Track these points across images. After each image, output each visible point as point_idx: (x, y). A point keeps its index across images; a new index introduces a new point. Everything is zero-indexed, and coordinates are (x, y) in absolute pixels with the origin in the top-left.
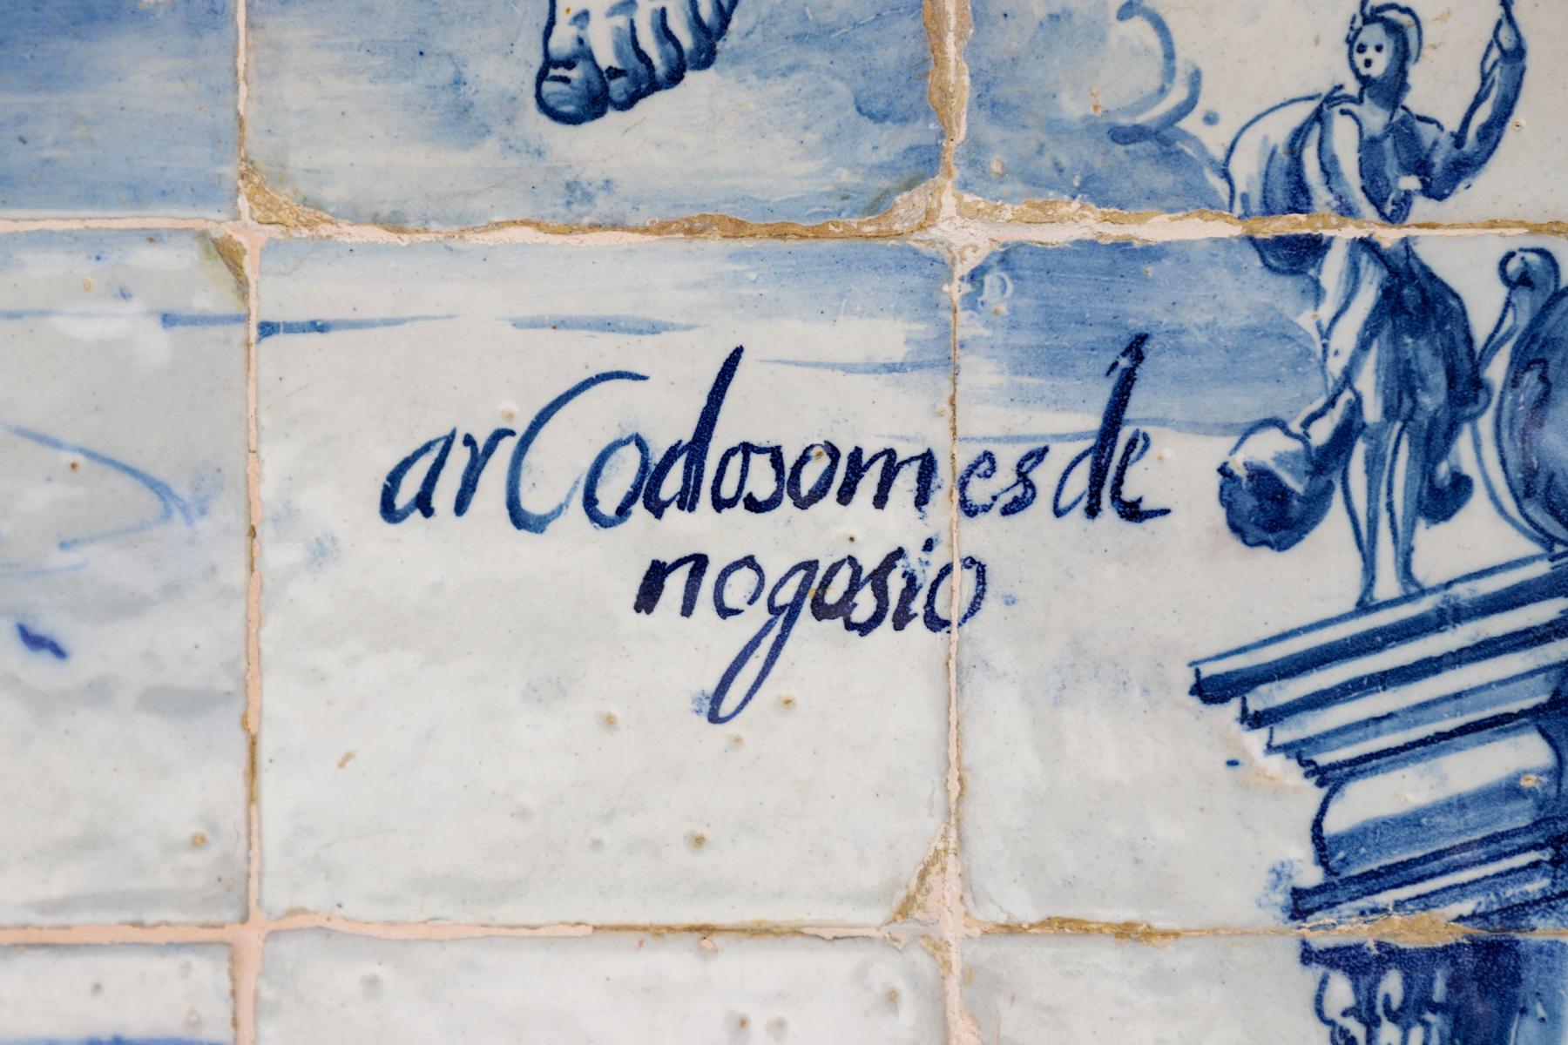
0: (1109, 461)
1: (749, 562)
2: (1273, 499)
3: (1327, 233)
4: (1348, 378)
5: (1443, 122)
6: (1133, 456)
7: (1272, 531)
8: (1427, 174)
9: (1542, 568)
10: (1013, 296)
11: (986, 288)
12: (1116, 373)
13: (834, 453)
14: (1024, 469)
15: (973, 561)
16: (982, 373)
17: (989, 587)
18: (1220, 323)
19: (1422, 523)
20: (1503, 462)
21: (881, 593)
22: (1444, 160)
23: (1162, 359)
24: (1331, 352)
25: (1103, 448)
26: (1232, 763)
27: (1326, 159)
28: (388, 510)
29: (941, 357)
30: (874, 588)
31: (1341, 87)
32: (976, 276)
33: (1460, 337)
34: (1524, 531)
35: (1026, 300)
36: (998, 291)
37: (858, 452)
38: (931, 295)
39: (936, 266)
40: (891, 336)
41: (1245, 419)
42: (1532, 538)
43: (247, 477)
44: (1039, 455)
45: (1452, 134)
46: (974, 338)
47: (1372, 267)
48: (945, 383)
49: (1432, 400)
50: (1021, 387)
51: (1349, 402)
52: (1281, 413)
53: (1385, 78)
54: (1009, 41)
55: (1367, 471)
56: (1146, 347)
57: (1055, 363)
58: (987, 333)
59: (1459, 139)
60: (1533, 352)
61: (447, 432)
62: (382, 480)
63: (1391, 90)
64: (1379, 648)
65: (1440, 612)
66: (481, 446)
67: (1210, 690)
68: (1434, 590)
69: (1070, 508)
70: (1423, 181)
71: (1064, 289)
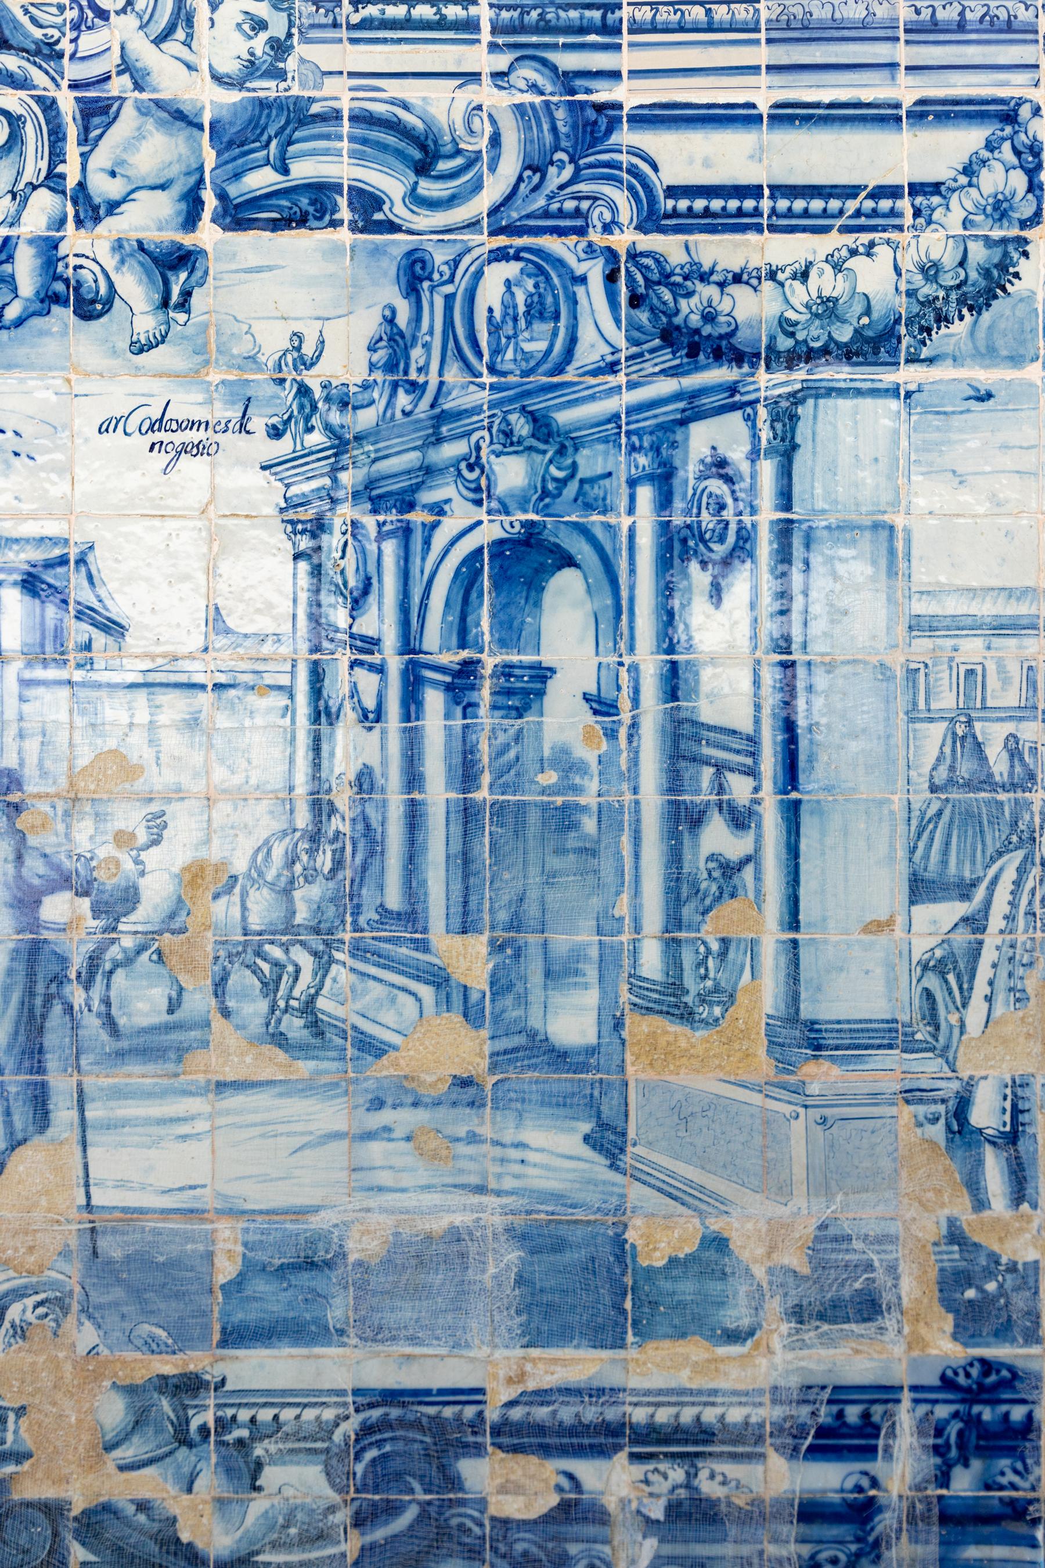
16: (218, 405)
29: (210, 402)
39: (210, 383)
40: (200, 397)
49: (307, 410)
54: (224, 338)
57: (233, 403)
63: (298, 349)
67: (264, 468)
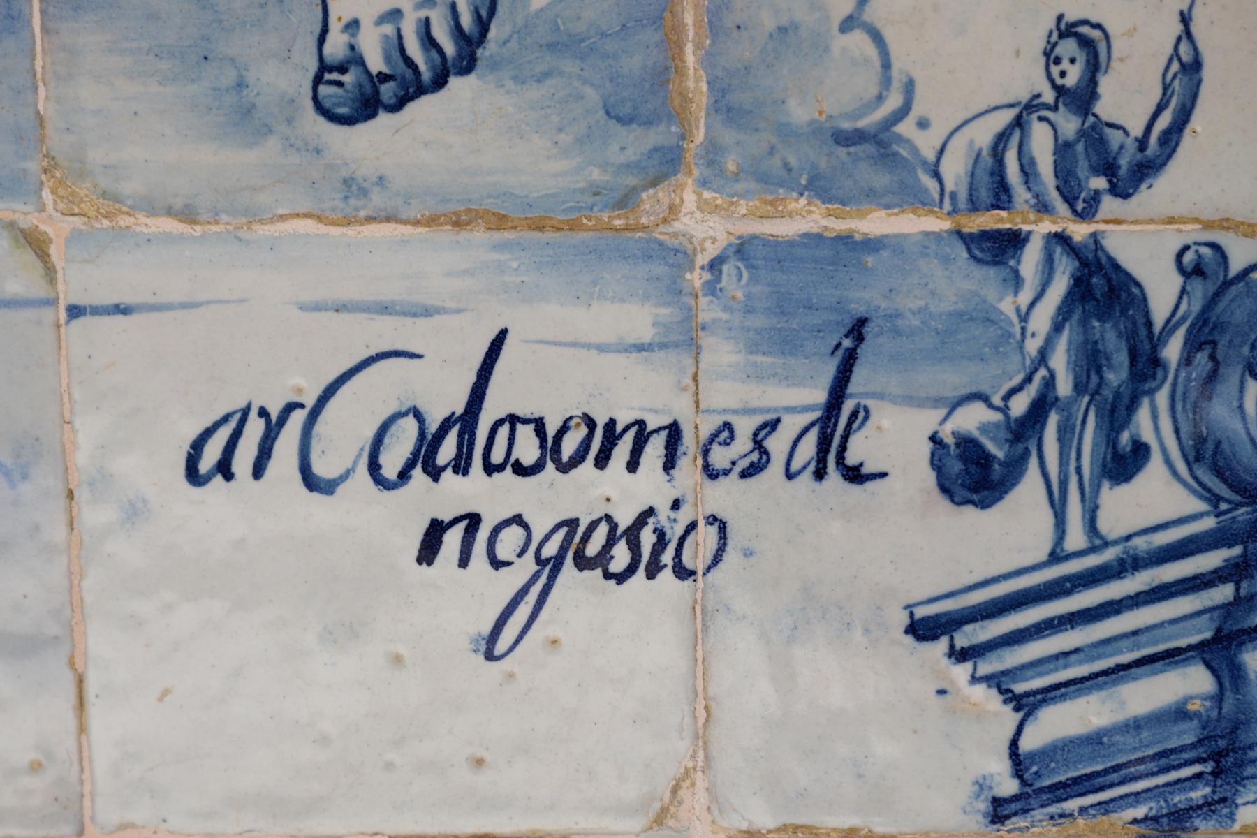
0: (834, 430)
1: (518, 520)
2: (978, 463)
3: (1026, 228)
4: (1043, 357)
5: (1128, 128)
6: (855, 426)
7: (976, 491)
8: (1114, 175)
9: (1209, 523)
10: (748, 284)
11: (725, 277)
12: (840, 353)
13: (591, 424)
14: (759, 438)
15: (715, 519)
16: (721, 353)
17: (730, 542)
18: (932, 308)
19: (1106, 485)
20: (1177, 431)
21: (635, 547)
22: (1129, 163)
23: (881, 340)
24: (1028, 334)
25: (829, 418)
26: (942, 692)
27: (1025, 161)
28: (193, 475)
29: (684, 339)
30: (628, 542)
31: (1039, 96)
32: (715, 265)
33: (1141, 320)
34: (1194, 492)
35: (759, 288)
36: (734, 279)
37: (612, 423)
38: (675, 282)
39: (680, 256)
40: (640, 319)
41: (951, 393)
42: (1201, 497)
43: (63, 445)
44: (773, 425)
45: (1136, 139)
46: (714, 321)
47: (1064, 259)
48: (688, 361)
49: (1116, 376)
50: (755, 364)
51: (1044, 378)
52: (984, 388)
53: (1078, 87)
55: (1059, 440)
56: (868, 330)
58: (725, 316)
59: (1142, 144)
60: (1204, 334)
61: (243, 405)
62: (186, 448)
63: (1082, 99)
64: (1068, 593)
65: (1121, 561)
66: (274, 417)
68: (1115, 542)
69: (799, 472)
70: (1110, 182)
71: (793, 277)
